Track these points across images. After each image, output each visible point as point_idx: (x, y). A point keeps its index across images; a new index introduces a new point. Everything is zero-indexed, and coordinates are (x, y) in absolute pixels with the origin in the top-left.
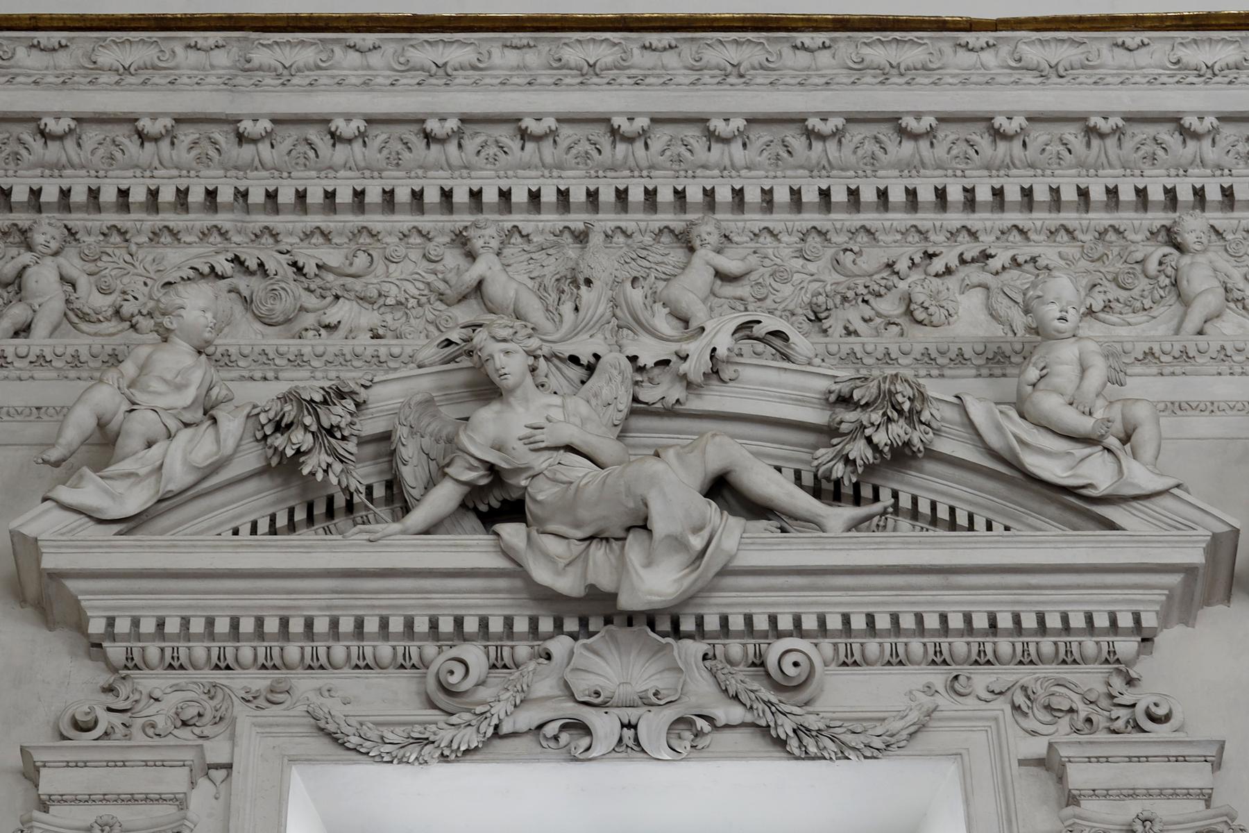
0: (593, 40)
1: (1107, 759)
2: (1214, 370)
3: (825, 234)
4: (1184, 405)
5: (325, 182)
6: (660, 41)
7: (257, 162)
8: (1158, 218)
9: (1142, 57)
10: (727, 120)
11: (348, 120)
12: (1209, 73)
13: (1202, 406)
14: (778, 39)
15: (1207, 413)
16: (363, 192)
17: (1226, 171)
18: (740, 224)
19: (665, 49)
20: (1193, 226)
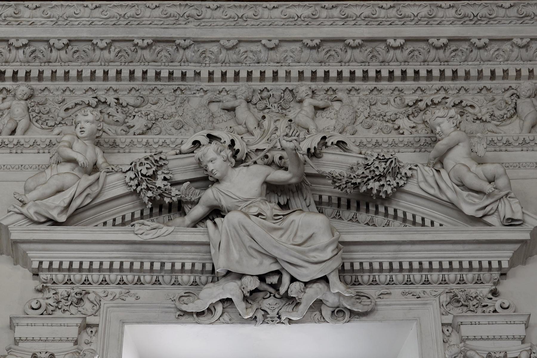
10: (185, 40)
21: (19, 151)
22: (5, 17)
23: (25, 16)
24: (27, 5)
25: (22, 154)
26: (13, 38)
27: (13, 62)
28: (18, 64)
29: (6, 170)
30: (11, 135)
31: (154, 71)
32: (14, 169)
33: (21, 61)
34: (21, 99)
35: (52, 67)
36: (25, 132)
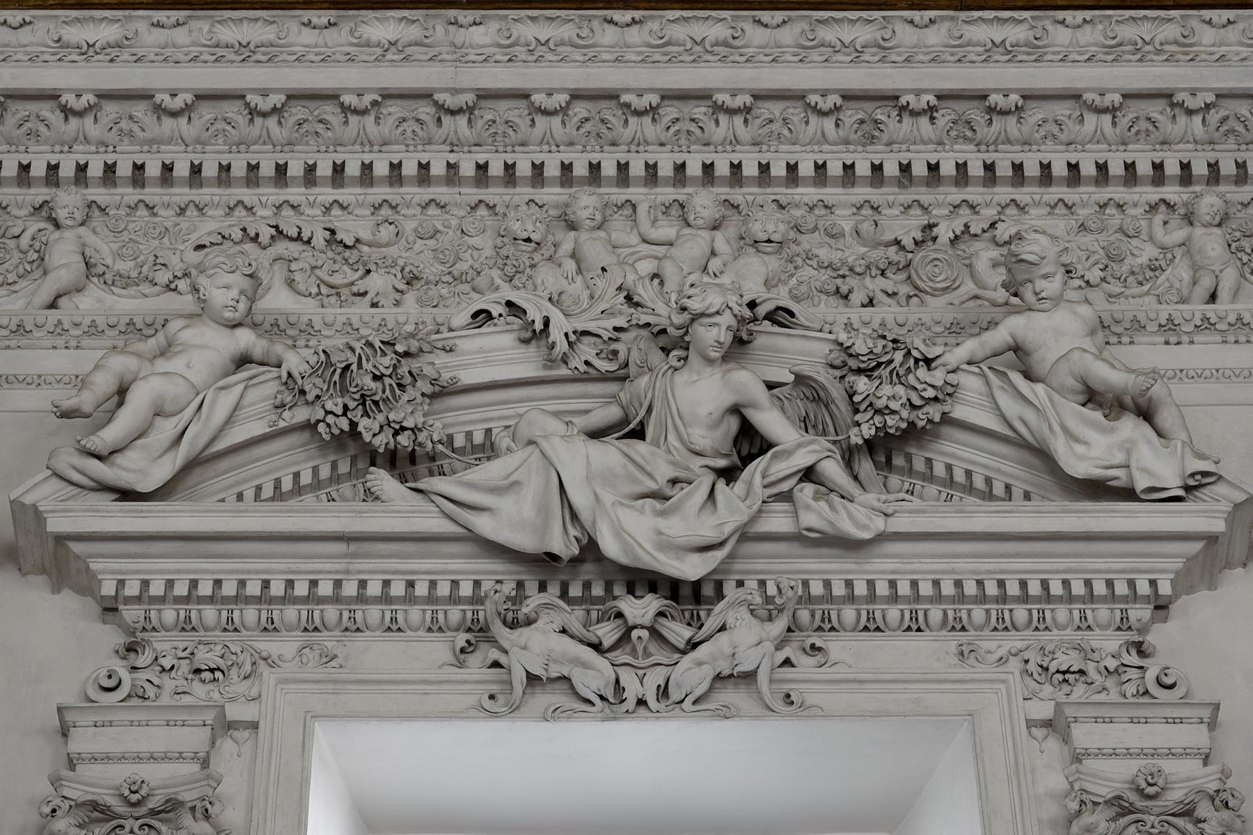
0: (92, 18)
1: (111, 724)
2: (48, 343)
3: (737, 207)
4: (12, 379)
5: (192, 156)
6: (168, 17)
7: (81, 137)
8: (39, 194)
9: (25, 35)
11: (174, 95)
12: (88, 51)
13: (29, 380)
14: (198, 18)
15: (33, 386)
16: (56, 167)
17: (111, 148)
18: (166, 198)
19: (21, 26)
20: (68, 201)
21: (1242, 339)
22: (1161, 44)
23: (1204, 42)
24: (1207, 19)
25: (1237, 346)
26: (1184, 90)
27: (1090, 142)
28: (1190, 146)
29: (1186, 380)
30: (1207, 303)
31: (869, 165)
32: (1241, 379)
33: (1196, 142)
34: (1210, 225)
35: (872, 156)
36: (1235, 294)
